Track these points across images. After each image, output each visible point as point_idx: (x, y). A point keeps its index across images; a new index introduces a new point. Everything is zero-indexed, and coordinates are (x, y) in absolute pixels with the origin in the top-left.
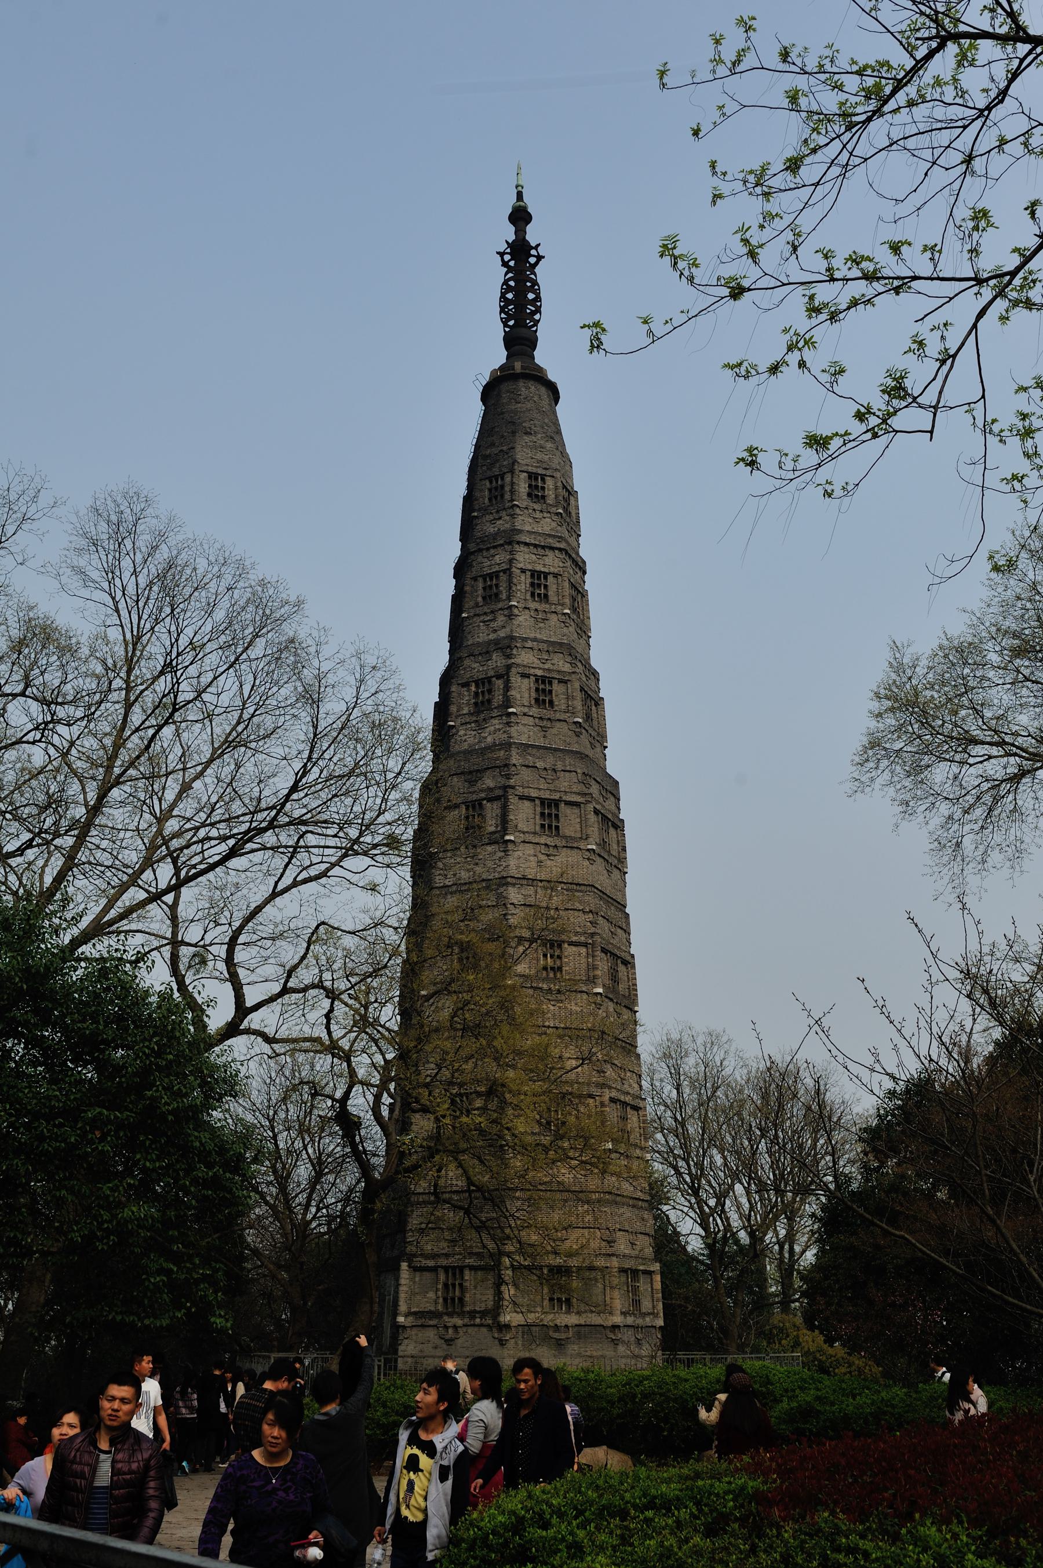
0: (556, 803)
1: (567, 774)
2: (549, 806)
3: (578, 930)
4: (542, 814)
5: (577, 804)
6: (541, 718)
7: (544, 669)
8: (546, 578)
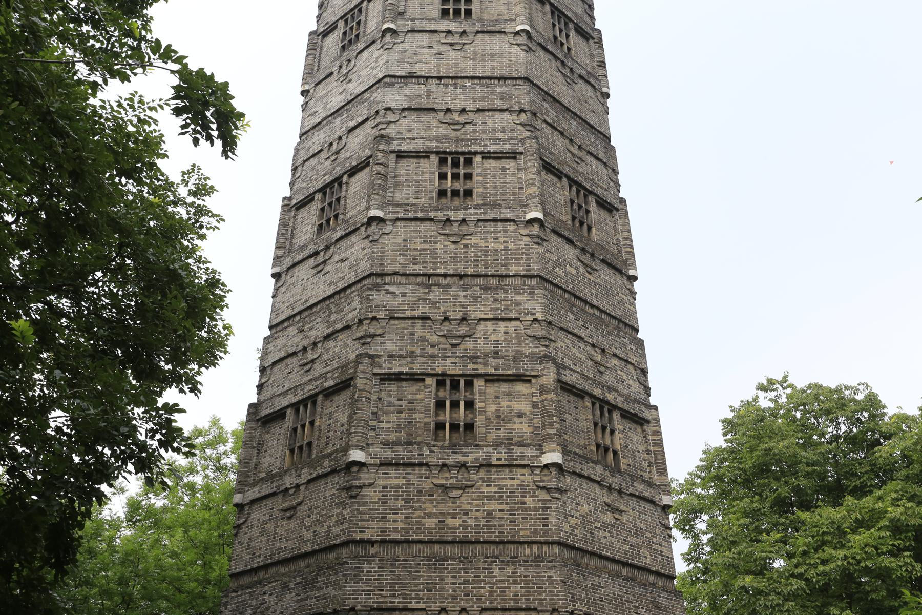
3: (501, 136)
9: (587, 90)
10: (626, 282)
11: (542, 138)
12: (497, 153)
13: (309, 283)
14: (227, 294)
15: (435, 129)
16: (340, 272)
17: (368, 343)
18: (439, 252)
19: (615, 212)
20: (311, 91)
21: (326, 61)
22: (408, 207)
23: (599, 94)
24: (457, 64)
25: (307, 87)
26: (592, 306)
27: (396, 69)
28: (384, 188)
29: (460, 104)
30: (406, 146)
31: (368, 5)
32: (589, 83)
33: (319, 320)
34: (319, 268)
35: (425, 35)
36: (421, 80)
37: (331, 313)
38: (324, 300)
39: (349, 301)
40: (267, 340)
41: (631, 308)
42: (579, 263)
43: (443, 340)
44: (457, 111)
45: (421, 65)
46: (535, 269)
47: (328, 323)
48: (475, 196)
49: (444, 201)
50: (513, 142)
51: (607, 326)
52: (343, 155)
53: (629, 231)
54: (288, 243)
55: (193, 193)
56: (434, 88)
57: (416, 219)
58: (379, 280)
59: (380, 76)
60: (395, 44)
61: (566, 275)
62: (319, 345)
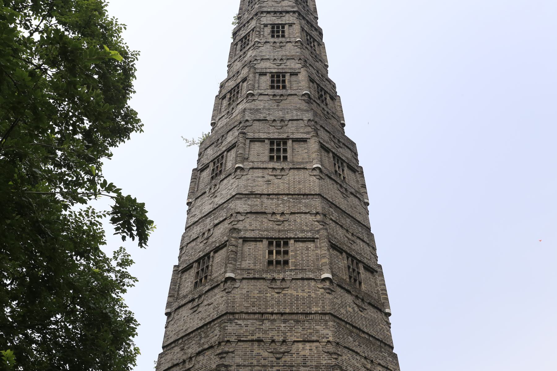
0: (285, 141)
1: (295, 122)
2: (278, 145)
3: (305, 228)
4: (272, 150)
5: (304, 140)
6: (274, 95)
7: (278, 69)
8: (283, 27)
9: (356, 201)
10: (384, 317)
11: (330, 229)
12: (303, 238)
13: (188, 319)
14: (137, 327)
15: (266, 224)
16: (207, 312)
17: (224, 357)
18: (268, 298)
19: (375, 273)
20: (193, 203)
21: (202, 186)
22: (250, 271)
23: (362, 203)
24: (278, 187)
25: (190, 200)
26: (364, 332)
27: (243, 190)
28: (236, 261)
29: (280, 209)
30: (248, 235)
31: (227, 154)
32: (357, 197)
33: (194, 342)
34: (195, 309)
35: (260, 171)
36: (258, 196)
37: (201, 338)
38: (197, 329)
39: (212, 330)
40: (161, 356)
41: (388, 333)
42: (355, 305)
43: (271, 355)
44: (279, 214)
45: (257, 187)
46: (327, 309)
47: (200, 345)
48: (290, 264)
49: (271, 267)
50: (313, 232)
51: (374, 345)
52: (211, 240)
53: (385, 285)
54: (176, 293)
55: (119, 265)
56: (265, 200)
57: (254, 279)
58: (231, 317)
59: (234, 194)
60: (242, 175)
61: (347, 312)
62: (193, 359)
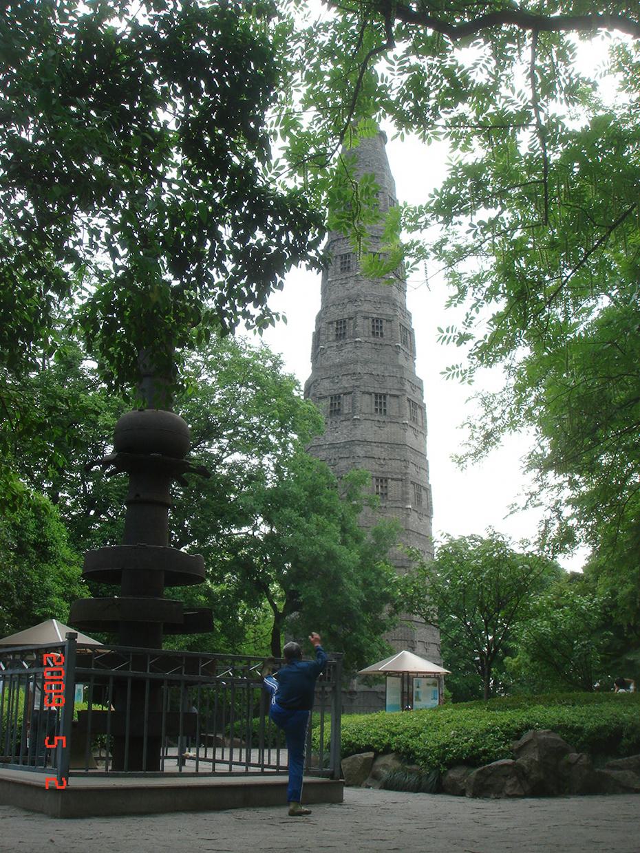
0: (385, 396)
5: (397, 396)
6: (376, 344)
7: (378, 314)
